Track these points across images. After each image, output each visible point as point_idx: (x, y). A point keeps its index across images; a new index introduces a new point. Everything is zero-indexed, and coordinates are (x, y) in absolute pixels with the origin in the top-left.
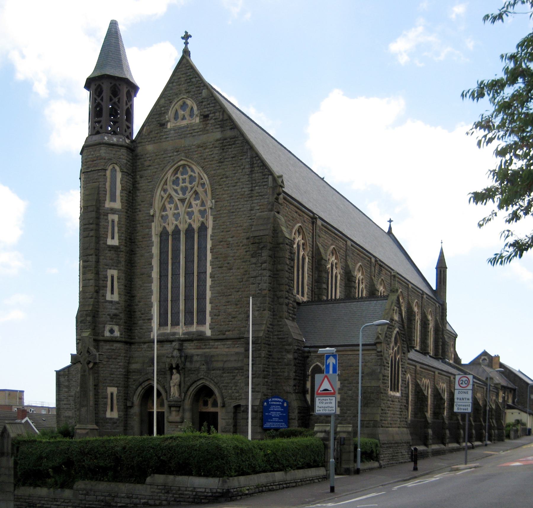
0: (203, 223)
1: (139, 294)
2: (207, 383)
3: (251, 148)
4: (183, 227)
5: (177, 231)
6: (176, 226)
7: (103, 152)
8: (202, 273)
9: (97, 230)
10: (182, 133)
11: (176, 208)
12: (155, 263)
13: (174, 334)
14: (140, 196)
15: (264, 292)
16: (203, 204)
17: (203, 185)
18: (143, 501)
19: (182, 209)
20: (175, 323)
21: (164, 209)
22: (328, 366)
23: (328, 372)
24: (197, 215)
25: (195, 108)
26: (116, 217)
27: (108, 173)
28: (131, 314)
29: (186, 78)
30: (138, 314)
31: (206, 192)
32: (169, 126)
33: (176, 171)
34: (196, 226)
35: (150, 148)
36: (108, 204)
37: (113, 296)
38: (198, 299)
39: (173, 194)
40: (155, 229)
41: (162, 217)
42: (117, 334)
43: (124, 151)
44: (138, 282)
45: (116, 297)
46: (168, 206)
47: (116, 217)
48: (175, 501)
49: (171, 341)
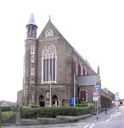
2: (56, 94)
4: (49, 59)
5: (48, 60)
6: (48, 58)
7: (30, 41)
8: (54, 69)
10: (49, 37)
11: (48, 54)
12: (42, 66)
13: (47, 83)
16: (54, 53)
17: (54, 49)
20: (48, 80)
21: (45, 54)
24: (53, 56)
26: (33, 56)
27: (32, 46)
28: (37, 78)
32: (46, 36)
34: (52, 58)
35: (41, 40)
37: (33, 74)
39: (47, 51)
41: (44, 56)
43: (35, 41)
46: (45, 54)
49: (47, 85)
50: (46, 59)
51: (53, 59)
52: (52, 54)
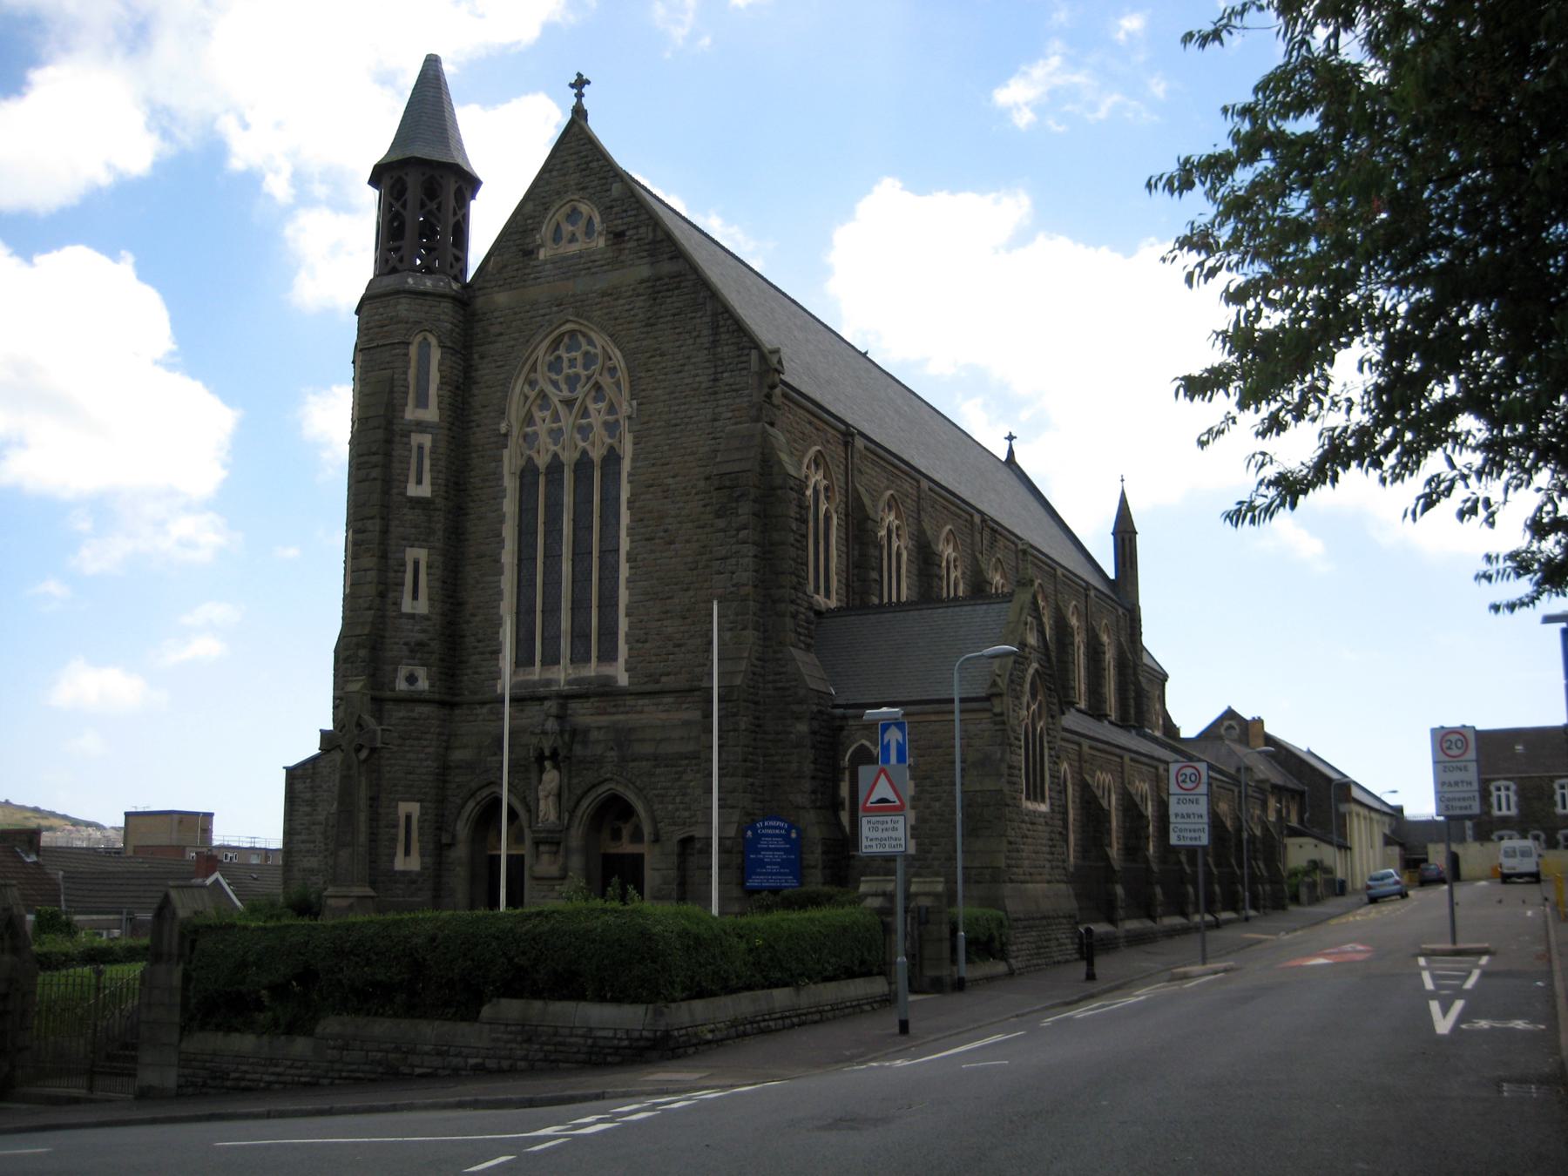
0: (611, 449)
2: (620, 790)
3: (713, 294)
4: (569, 457)
5: (556, 467)
6: (556, 455)
7: (403, 308)
8: (609, 551)
9: (386, 467)
10: (569, 268)
11: (556, 418)
12: (509, 532)
13: (548, 683)
16: (612, 409)
17: (612, 371)
18: (472, 1061)
19: (567, 421)
20: (551, 659)
21: (529, 420)
24: (598, 430)
25: (597, 219)
26: (427, 440)
27: (413, 350)
28: (455, 642)
31: (618, 384)
32: (542, 254)
34: (596, 454)
35: (502, 298)
36: (411, 413)
37: (416, 603)
38: (600, 607)
39: (550, 389)
41: (525, 436)
43: (446, 306)
45: (422, 607)
46: (538, 415)
48: (545, 1059)
49: (541, 699)
50: (542, 461)
51: (542, 468)
52: (597, 414)
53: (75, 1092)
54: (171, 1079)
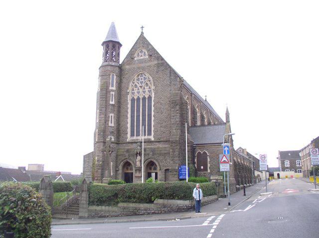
0: (150, 95)
1: (122, 123)
2: (153, 160)
3: (170, 67)
4: (141, 97)
5: (138, 99)
6: (138, 97)
7: (109, 68)
8: (150, 115)
9: (106, 98)
10: (141, 61)
11: (138, 89)
12: (129, 111)
13: (137, 140)
14: (123, 85)
15: (178, 122)
16: (150, 88)
17: (150, 81)
18: (152, 211)
19: (141, 90)
20: (138, 135)
21: (133, 90)
22: (225, 151)
23: (225, 153)
24: (147, 92)
25: (146, 52)
26: (113, 93)
27: (111, 76)
28: (119, 131)
29: (142, 42)
30: (121, 132)
31: (151, 83)
32: (135, 59)
33: (138, 76)
34: (147, 96)
35: (127, 67)
36: (111, 88)
37: (112, 124)
38: (148, 125)
39: (137, 84)
40: (129, 97)
41: (132, 93)
42: (113, 140)
43: (117, 68)
44: (122, 119)
45: (113, 125)
46: (135, 89)
47: (113, 93)
48: (168, 211)
49: (136, 143)
50: (136, 98)
51: (147, 97)
52: (147, 89)
53: (64, 217)
54: (86, 215)
